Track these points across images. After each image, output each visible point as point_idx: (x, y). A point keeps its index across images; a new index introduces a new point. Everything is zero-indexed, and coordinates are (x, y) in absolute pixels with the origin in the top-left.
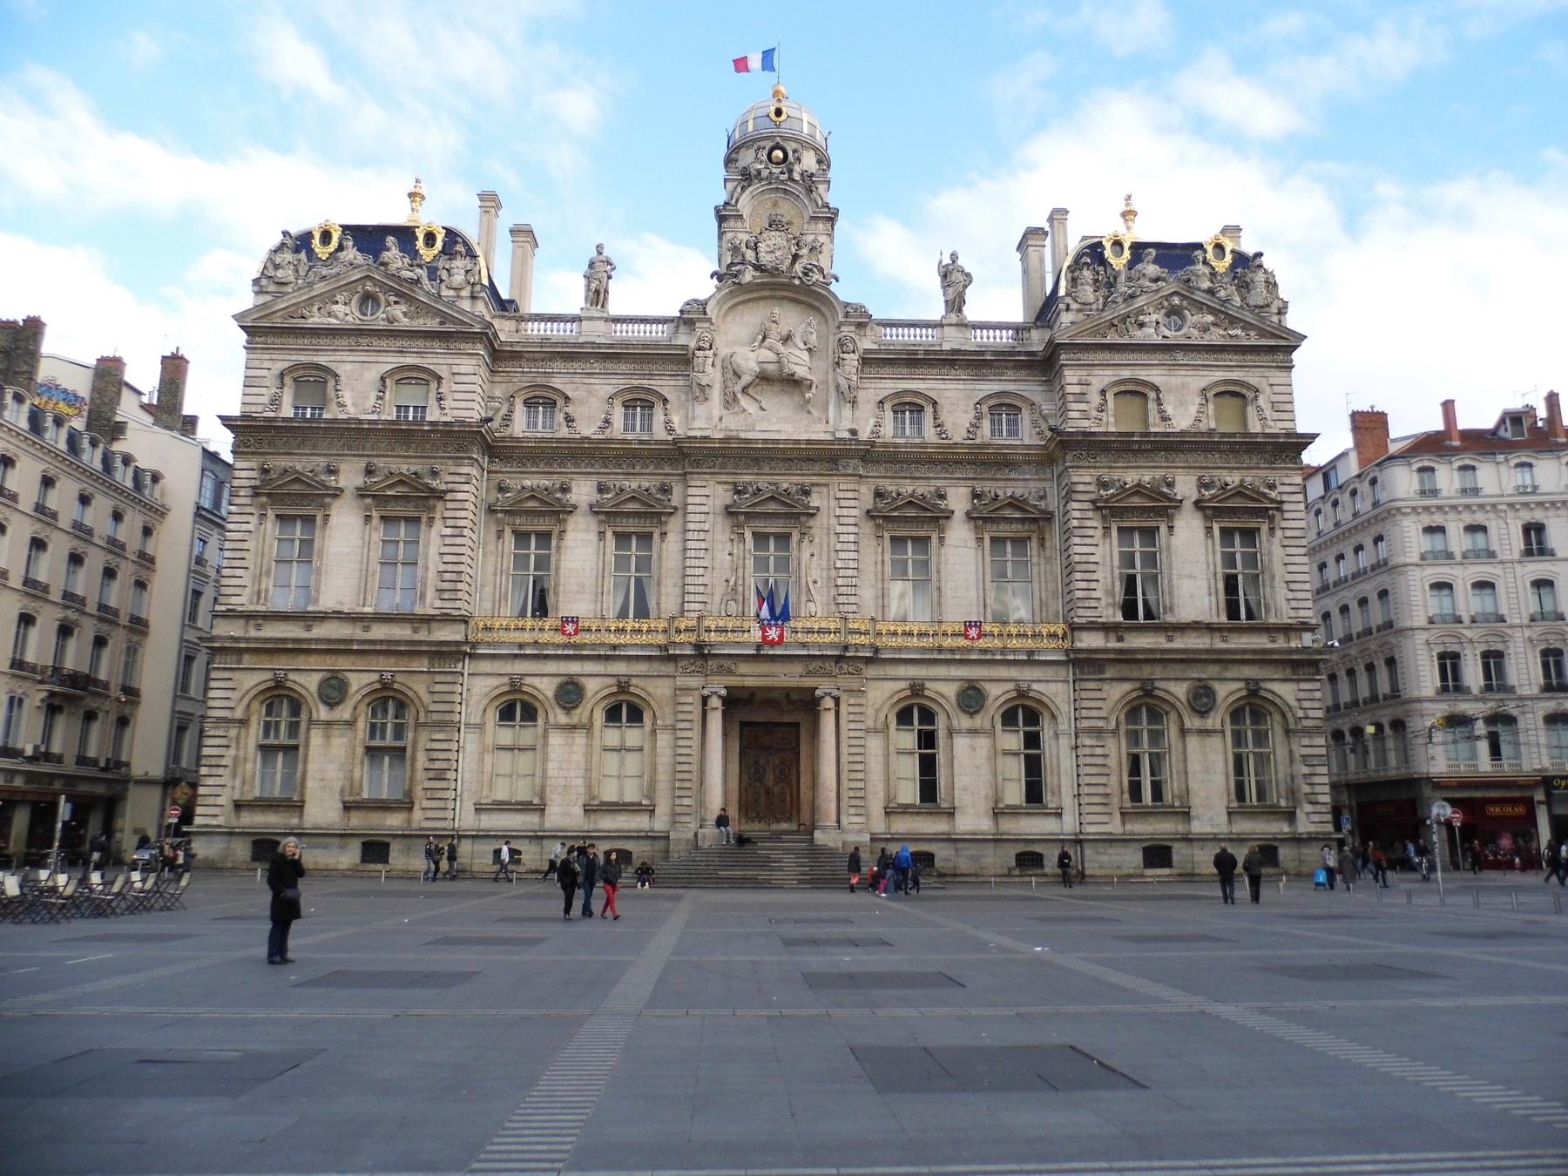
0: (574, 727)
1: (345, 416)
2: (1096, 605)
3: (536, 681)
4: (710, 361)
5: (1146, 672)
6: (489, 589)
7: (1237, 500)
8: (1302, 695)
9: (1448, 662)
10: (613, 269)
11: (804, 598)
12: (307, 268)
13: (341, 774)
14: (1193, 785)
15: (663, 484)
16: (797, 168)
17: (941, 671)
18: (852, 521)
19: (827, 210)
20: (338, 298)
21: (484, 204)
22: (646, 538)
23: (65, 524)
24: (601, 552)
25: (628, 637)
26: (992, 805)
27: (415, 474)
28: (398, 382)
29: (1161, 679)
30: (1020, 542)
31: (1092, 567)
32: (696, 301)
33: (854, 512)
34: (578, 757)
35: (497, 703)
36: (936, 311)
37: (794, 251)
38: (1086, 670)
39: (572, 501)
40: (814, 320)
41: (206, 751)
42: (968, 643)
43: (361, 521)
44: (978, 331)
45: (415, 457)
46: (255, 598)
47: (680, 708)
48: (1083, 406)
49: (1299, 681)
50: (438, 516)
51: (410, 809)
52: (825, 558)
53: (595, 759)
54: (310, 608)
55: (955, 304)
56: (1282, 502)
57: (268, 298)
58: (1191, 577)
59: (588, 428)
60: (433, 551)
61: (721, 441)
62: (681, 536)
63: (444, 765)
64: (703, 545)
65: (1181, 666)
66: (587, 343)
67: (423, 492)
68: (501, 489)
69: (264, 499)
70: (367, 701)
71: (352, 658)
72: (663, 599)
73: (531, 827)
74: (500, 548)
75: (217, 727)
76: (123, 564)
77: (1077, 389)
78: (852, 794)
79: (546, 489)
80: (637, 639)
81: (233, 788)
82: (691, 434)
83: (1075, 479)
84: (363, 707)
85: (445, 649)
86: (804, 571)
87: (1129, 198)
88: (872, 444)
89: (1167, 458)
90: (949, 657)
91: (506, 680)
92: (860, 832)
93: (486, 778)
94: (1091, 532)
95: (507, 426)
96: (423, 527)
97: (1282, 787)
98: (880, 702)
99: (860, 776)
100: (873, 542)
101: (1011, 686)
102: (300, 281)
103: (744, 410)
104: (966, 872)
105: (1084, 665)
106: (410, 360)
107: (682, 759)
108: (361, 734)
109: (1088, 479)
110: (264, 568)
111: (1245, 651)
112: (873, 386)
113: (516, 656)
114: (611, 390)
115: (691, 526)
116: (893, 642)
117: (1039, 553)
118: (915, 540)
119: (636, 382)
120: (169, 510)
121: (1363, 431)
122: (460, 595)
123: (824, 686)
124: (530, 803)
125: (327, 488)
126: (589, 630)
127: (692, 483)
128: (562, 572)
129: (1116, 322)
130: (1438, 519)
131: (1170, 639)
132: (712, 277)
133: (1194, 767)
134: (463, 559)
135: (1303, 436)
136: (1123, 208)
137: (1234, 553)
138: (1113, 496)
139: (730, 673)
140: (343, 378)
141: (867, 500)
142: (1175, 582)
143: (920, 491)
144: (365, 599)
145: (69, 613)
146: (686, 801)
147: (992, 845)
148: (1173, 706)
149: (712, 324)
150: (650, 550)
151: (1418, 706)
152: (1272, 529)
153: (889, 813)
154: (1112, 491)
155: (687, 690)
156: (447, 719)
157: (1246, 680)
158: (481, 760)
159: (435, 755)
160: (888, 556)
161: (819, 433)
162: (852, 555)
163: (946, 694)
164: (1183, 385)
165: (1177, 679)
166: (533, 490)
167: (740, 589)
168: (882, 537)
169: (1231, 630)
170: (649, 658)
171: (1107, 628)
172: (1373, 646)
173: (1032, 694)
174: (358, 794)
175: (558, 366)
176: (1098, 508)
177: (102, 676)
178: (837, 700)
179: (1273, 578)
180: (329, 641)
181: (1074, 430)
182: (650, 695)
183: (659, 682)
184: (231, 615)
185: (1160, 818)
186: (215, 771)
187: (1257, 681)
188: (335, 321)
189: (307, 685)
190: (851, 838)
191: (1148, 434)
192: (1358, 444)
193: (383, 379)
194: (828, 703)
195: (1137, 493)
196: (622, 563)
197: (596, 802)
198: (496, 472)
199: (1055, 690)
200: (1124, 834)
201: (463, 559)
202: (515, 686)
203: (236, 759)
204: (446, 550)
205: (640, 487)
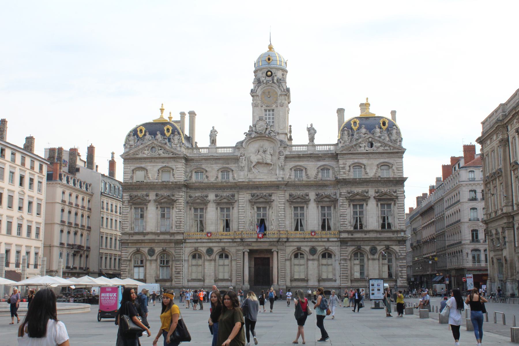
0: (211, 260)
1: (149, 181)
3: (201, 249)
4: (244, 160)
5: (359, 243)
6: (188, 224)
8: (400, 249)
9: (475, 233)
10: (217, 133)
11: (270, 224)
13: (155, 273)
14: (370, 273)
16: (275, 78)
17: (305, 244)
18: (283, 203)
19: (284, 92)
20: (146, 149)
21: (182, 116)
22: (228, 209)
23: (74, 206)
26: (318, 278)
27: (168, 195)
29: (363, 245)
30: (329, 208)
31: (345, 215)
33: (283, 200)
34: (212, 268)
35: (192, 254)
36: (306, 141)
37: (266, 127)
38: (343, 243)
40: (272, 145)
42: (312, 236)
47: (237, 255)
48: (344, 171)
50: (175, 206)
51: (172, 281)
52: (276, 213)
53: (217, 268)
54: (144, 232)
55: (312, 139)
56: (398, 197)
58: (372, 217)
59: (212, 179)
60: (174, 215)
61: (247, 182)
64: (243, 211)
65: (369, 242)
66: (211, 156)
67: (170, 200)
68: (190, 197)
69: (131, 204)
70: (160, 254)
72: (233, 225)
73: (201, 285)
76: (85, 211)
77: (342, 166)
79: (202, 197)
80: (226, 237)
82: (239, 180)
84: (159, 256)
85: (178, 241)
86: (270, 217)
87: (367, 99)
88: (288, 182)
89: (366, 185)
90: (307, 240)
93: (190, 273)
94: (345, 206)
96: (171, 209)
97: (395, 273)
98: (289, 252)
99: (284, 272)
101: (324, 247)
102: (136, 144)
105: (343, 242)
107: (239, 268)
109: (345, 191)
110: (133, 221)
111: (385, 238)
112: (288, 164)
113: (196, 242)
115: (240, 206)
116: (292, 237)
117: (334, 211)
118: (300, 207)
119: (225, 166)
120: (93, 194)
121: (467, 152)
122: (181, 227)
123: (274, 249)
124: (201, 279)
125: (147, 200)
127: (240, 194)
128: (207, 218)
130: (474, 188)
131: (365, 235)
132: (244, 134)
133: (371, 268)
134: (181, 217)
135: (403, 178)
137: (385, 211)
138: (351, 196)
139: (250, 246)
140: (149, 171)
142: (367, 219)
143: (301, 194)
145: (76, 229)
146: (239, 279)
148: (366, 253)
149: (244, 148)
150: (230, 212)
151: (464, 246)
153: (291, 281)
154: (351, 194)
155: (238, 250)
157: (386, 245)
158: (188, 269)
159: (177, 268)
165: (367, 245)
166: (198, 197)
167: (253, 222)
168: (291, 207)
169: (382, 232)
171: (348, 232)
173: (329, 249)
174: (159, 278)
175: (204, 161)
176: (347, 199)
177: (83, 245)
178: (277, 252)
180: (150, 240)
181: (341, 178)
182: (230, 251)
183: (232, 248)
185: (361, 282)
186: (124, 273)
187: (388, 246)
188: (145, 155)
190: (281, 287)
191: (360, 179)
193: (159, 170)
194: (275, 254)
195: (358, 195)
197: (217, 279)
199: (335, 248)
201: (181, 217)
202: (196, 250)
203: (129, 269)
204: (177, 215)
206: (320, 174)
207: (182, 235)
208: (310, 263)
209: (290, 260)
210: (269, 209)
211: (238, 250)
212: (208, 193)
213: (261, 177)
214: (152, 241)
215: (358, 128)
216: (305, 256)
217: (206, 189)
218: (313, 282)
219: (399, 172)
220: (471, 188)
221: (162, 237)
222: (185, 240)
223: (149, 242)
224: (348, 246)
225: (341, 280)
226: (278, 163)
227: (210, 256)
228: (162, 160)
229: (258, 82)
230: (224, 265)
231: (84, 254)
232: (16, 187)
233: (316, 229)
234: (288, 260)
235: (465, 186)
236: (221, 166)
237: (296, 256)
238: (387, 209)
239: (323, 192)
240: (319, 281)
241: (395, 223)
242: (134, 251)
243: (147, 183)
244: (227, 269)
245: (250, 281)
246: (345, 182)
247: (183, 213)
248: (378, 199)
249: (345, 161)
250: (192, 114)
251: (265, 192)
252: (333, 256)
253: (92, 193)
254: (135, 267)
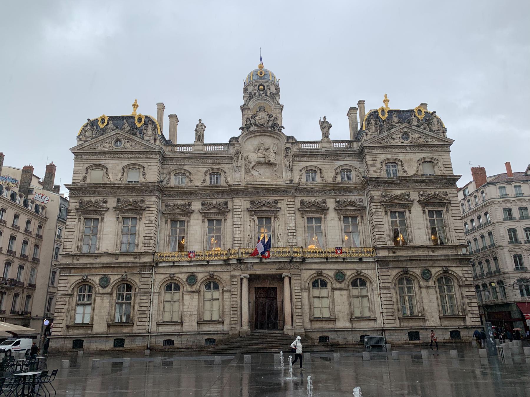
0: (193, 292)
1: (110, 182)
2: (384, 240)
3: (179, 275)
5: (404, 265)
7: (433, 200)
8: (464, 272)
9: (518, 258)
11: (276, 241)
12: (96, 131)
13: (107, 313)
14: (425, 308)
15: (225, 202)
17: (328, 266)
18: (293, 212)
21: (159, 107)
24: (203, 227)
25: (213, 257)
26: (349, 317)
27: (135, 201)
28: (128, 170)
30: (354, 218)
31: (382, 226)
32: (234, 138)
33: (293, 209)
35: (165, 284)
36: (319, 137)
37: (268, 119)
39: (192, 209)
40: (276, 141)
43: (115, 219)
44: (335, 144)
45: (135, 196)
46: (76, 249)
47: (232, 283)
48: (375, 168)
49: (462, 267)
50: (143, 216)
51: (133, 326)
52: (284, 226)
53: (201, 304)
54: (96, 252)
55: (326, 134)
56: (451, 200)
57: (82, 142)
62: (232, 220)
63: (145, 308)
64: (240, 223)
69: (80, 213)
70: (117, 286)
71: (112, 269)
73: (178, 331)
74: (166, 227)
75: (60, 298)
76: (30, 239)
77: (372, 162)
78: (297, 314)
80: (216, 258)
81: (67, 320)
82: (234, 184)
83: (373, 195)
84: (115, 288)
87: (386, 96)
91: (168, 275)
92: (300, 329)
94: (380, 214)
95: (168, 183)
96: (138, 221)
97: (460, 308)
99: (300, 307)
100: (301, 220)
101: (354, 271)
102: (94, 136)
103: (252, 175)
104: (341, 344)
105: (383, 263)
106: (133, 162)
107: (234, 303)
108: (115, 298)
109: (378, 194)
112: (298, 164)
113: (172, 266)
114: (205, 169)
115: (235, 216)
119: (214, 166)
122: (151, 245)
123: (285, 273)
125: (103, 208)
126: (199, 255)
127: (235, 201)
128: (189, 235)
129: (384, 138)
130: (508, 205)
131: (413, 252)
132: (240, 129)
136: (384, 99)
138: (387, 200)
140: (109, 169)
141: (298, 205)
142: (412, 231)
143: (317, 201)
144: (116, 247)
145: (9, 257)
146: (235, 319)
147: (351, 332)
149: (240, 145)
151: (507, 275)
152: (447, 210)
153: (311, 321)
154: (387, 198)
156: (147, 291)
158: (159, 306)
159: (142, 305)
160: (306, 225)
161: (279, 182)
162: (294, 225)
163: (330, 275)
164: (410, 159)
167: (253, 238)
170: (221, 265)
171: (389, 249)
172: (488, 253)
173: (362, 274)
175: (186, 161)
177: (22, 280)
179: (449, 228)
180: (103, 263)
182: (221, 278)
183: (225, 274)
184: (68, 255)
188: (106, 149)
189: (95, 280)
190: (297, 331)
192: (475, 179)
193: (123, 169)
196: (210, 230)
197: (202, 320)
198: (164, 200)
200: (400, 327)
201: (152, 231)
202: (172, 277)
203: (69, 310)
205: (216, 203)
206: (339, 177)
207: (152, 256)
208: (337, 293)
209: (308, 289)
210: (274, 221)
211: (232, 276)
212: (192, 201)
213: (263, 180)
214: (107, 266)
215: (387, 117)
216: (329, 285)
217: (188, 196)
218: (343, 323)
219: (448, 169)
220: (504, 206)
221: (121, 259)
222: (157, 263)
223: (102, 267)
224: (390, 268)
225: (385, 318)
226: (284, 163)
227: (191, 285)
228: (129, 156)
229: (249, 95)
230: (212, 300)
231: (23, 292)
233: (339, 246)
234: (305, 289)
235: (497, 204)
236: (210, 166)
237: (315, 284)
238: (437, 217)
239: (346, 199)
240: (352, 320)
241: (451, 236)
242: (79, 281)
243: (105, 184)
244: (216, 305)
245: (250, 322)
246: (378, 182)
247: (155, 226)
248: (424, 204)
249: (374, 157)
250: (174, 118)
251: (269, 199)
252: (368, 284)
253: (46, 218)
254: (77, 305)
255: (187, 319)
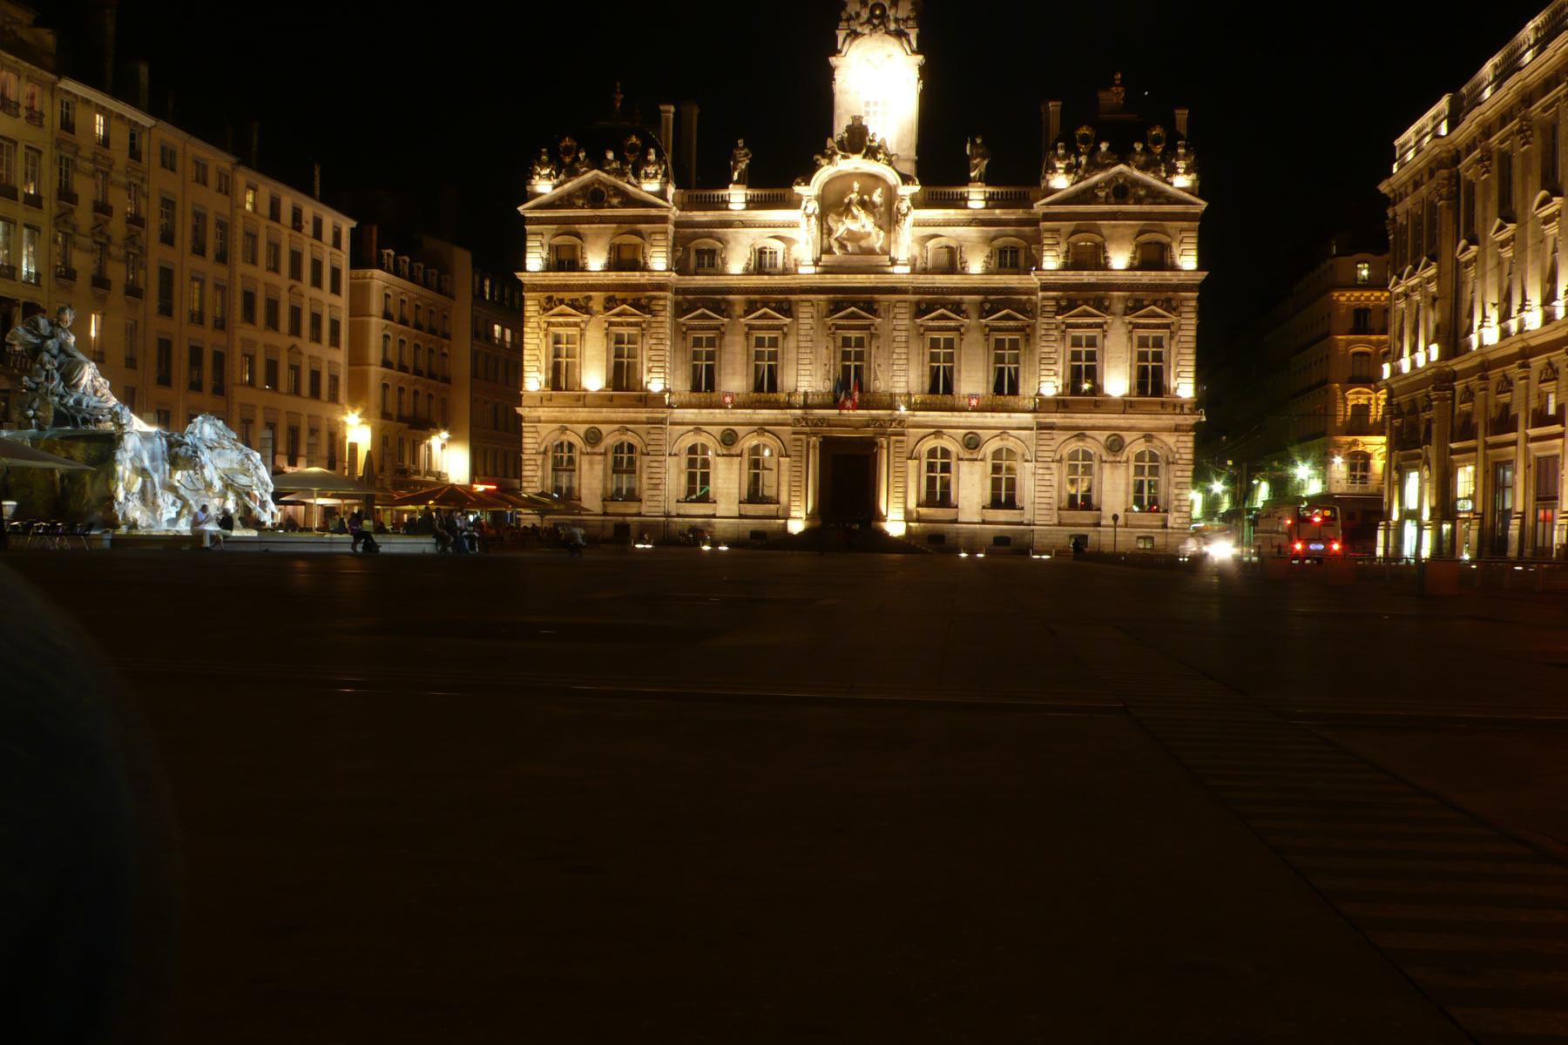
8: (1180, 445)
13: (601, 486)
14: (1104, 498)
18: (904, 327)
30: (1014, 344)
41: (525, 473)
62: (795, 338)
115: (802, 333)
133: (1106, 486)
158: (679, 478)
159: (653, 476)
186: (531, 485)
232: (283, 280)
255: (723, 500)
